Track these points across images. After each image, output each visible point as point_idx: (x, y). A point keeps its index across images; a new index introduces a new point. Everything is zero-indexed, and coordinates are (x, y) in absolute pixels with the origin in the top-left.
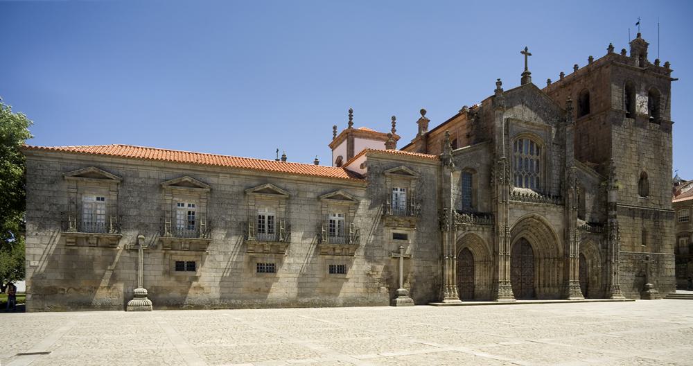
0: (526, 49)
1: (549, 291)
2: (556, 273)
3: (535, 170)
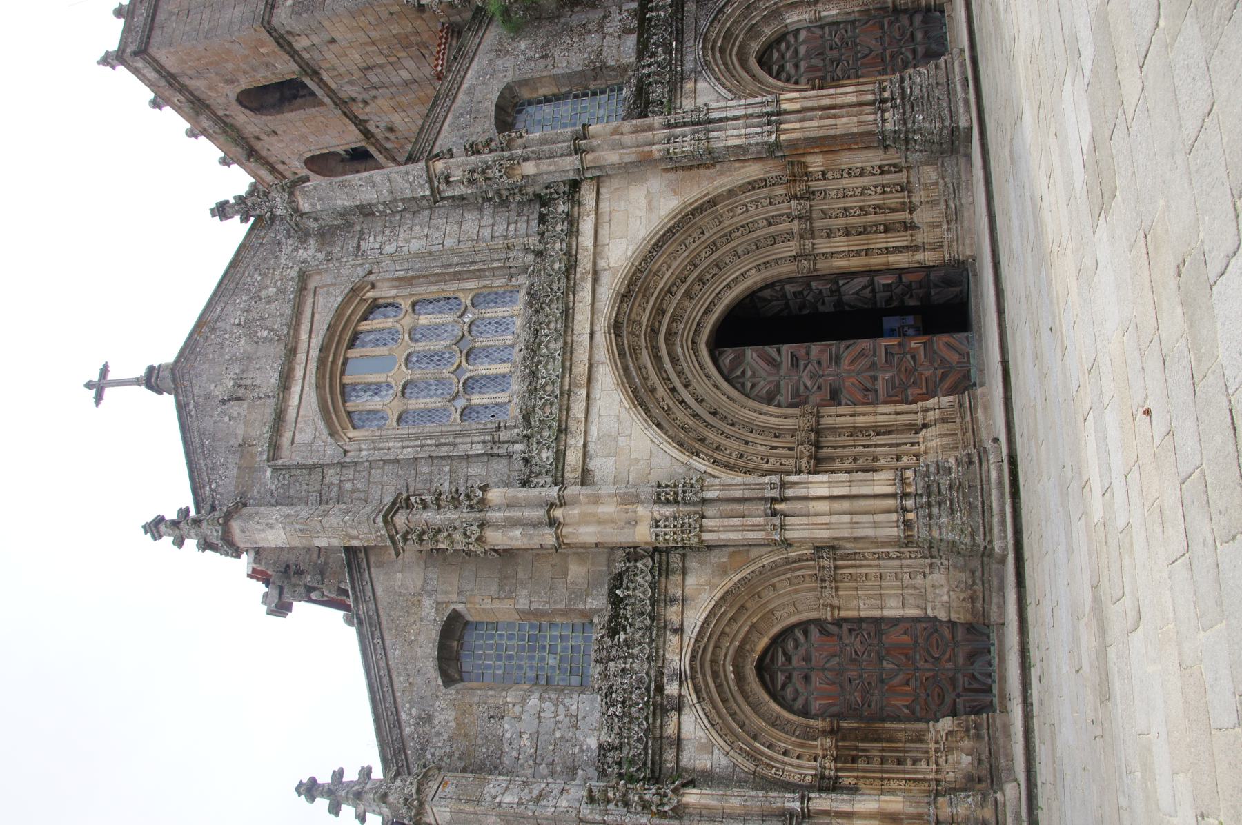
0: (89, 385)
1: (933, 203)
2: (848, 183)
3: (448, 318)
